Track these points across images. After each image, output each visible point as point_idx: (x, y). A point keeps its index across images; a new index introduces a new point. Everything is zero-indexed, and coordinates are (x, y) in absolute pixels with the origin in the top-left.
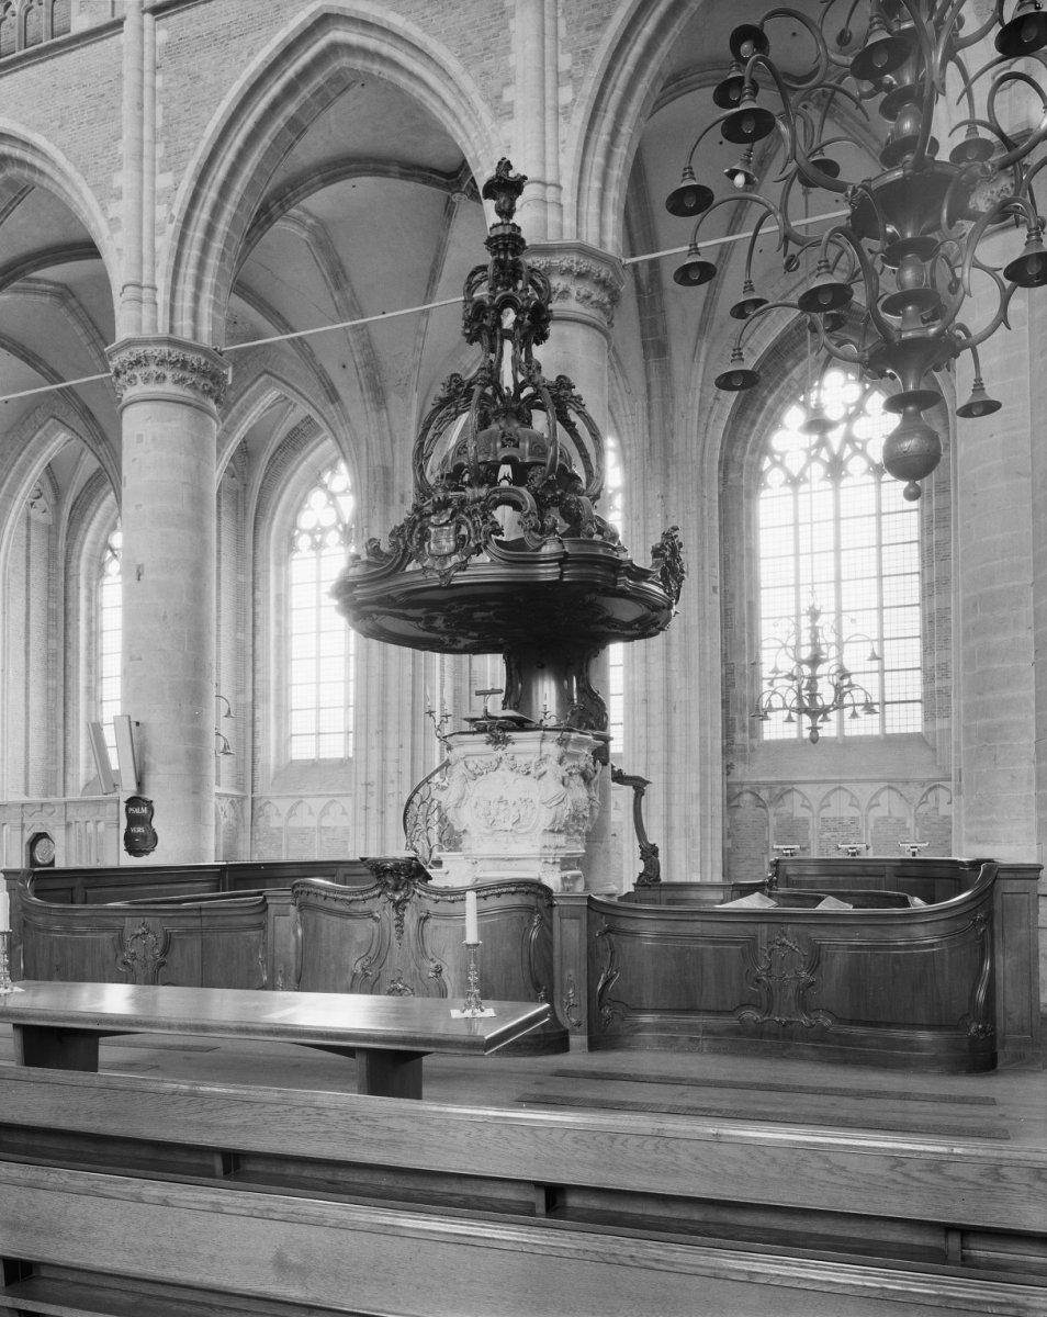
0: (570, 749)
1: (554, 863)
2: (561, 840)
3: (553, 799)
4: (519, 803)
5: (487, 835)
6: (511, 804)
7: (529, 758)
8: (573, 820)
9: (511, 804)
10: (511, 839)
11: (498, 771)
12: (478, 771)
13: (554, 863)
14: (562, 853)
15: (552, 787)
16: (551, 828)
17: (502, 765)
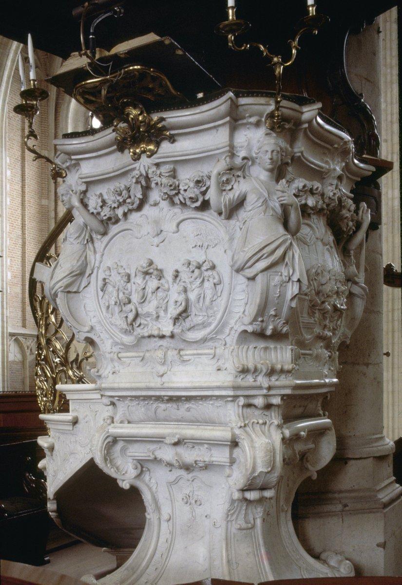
0: (300, 147)
1: (268, 407)
2: (283, 355)
3: (257, 256)
4: (184, 276)
5: (127, 348)
6: (169, 275)
7: (205, 169)
8: (311, 314)
9: (169, 275)
10: (172, 354)
11: (147, 209)
12: (106, 213)
13: (268, 407)
14: (286, 384)
15: (258, 229)
16: (256, 327)
17: (155, 195)
